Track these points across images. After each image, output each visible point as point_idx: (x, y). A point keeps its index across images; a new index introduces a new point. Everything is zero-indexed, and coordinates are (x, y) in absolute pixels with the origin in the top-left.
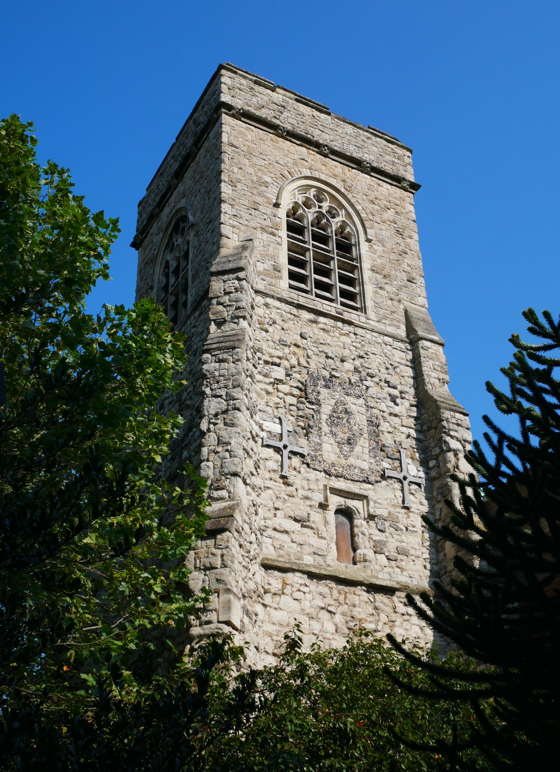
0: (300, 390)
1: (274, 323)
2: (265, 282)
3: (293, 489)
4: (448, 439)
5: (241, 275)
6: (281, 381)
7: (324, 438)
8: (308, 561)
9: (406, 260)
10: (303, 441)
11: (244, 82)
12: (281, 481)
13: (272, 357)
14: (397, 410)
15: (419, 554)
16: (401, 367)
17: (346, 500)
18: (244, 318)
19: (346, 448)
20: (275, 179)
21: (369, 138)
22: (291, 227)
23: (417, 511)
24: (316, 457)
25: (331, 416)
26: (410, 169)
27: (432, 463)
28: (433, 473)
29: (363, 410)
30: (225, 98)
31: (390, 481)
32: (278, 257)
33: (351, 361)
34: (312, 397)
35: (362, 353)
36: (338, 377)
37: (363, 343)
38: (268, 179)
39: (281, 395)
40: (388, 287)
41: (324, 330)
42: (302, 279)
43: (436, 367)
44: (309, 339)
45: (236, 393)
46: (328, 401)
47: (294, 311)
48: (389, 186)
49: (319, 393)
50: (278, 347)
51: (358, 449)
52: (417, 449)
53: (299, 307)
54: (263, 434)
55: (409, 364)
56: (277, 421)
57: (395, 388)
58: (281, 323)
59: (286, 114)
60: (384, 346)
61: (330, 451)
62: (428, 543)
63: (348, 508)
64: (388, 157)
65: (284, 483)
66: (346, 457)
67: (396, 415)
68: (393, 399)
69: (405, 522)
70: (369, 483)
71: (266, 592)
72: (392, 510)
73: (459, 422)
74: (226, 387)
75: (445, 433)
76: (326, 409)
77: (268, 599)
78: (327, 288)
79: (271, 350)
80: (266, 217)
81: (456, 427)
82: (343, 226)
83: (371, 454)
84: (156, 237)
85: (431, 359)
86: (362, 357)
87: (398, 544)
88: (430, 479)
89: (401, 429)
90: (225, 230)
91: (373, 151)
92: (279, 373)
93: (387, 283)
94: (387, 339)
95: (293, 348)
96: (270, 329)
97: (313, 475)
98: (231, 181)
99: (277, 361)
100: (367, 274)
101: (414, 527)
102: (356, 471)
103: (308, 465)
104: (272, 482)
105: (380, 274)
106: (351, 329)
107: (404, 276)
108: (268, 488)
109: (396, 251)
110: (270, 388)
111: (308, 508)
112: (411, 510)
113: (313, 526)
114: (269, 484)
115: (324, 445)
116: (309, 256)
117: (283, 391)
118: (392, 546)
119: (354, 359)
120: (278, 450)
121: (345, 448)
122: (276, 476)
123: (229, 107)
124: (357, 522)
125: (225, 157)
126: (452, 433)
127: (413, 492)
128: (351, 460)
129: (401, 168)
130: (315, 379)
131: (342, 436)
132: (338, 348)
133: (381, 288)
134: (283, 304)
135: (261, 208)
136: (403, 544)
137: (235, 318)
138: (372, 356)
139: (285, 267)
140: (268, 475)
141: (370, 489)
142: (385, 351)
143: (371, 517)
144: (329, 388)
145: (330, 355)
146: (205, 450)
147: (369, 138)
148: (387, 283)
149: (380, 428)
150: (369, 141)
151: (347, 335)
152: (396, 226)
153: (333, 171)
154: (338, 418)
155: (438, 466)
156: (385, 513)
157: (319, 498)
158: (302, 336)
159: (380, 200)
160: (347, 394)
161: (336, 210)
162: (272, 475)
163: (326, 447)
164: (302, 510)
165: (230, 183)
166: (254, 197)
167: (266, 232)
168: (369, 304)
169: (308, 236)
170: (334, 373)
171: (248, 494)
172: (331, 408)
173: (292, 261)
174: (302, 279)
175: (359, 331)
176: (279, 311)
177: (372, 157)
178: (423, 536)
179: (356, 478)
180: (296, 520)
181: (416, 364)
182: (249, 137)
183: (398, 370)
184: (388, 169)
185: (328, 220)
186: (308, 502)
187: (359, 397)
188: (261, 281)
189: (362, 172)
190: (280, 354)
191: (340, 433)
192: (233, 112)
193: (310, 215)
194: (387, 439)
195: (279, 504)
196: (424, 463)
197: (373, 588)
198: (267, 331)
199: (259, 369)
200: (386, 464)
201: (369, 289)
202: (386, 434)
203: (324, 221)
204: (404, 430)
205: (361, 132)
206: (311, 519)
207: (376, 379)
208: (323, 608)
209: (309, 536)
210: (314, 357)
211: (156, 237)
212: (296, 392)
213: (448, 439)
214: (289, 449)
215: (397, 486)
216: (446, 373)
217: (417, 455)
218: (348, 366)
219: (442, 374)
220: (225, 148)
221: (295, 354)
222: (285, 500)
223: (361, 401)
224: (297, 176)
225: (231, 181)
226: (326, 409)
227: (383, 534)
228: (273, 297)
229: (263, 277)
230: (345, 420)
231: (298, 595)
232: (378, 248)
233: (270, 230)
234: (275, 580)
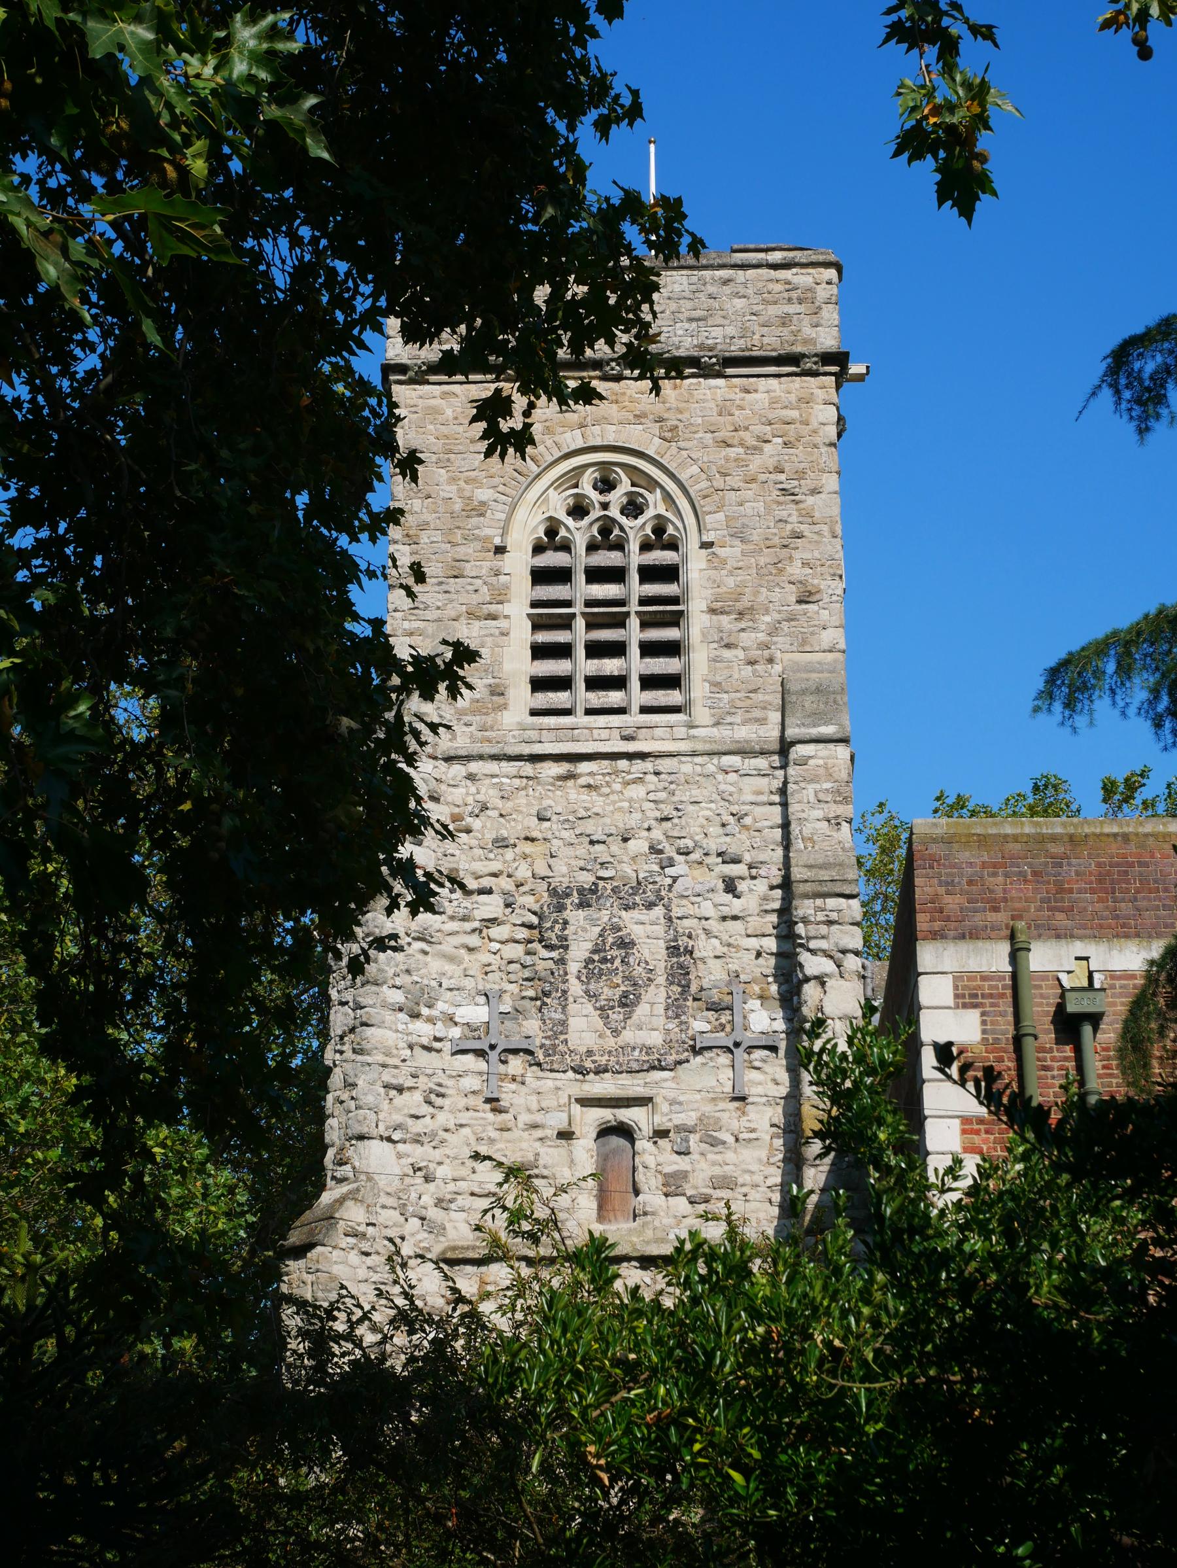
0: (530, 927)
1: (484, 808)
2: (472, 729)
3: (509, 1116)
6: (493, 921)
7: (572, 1008)
9: (797, 555)
12: (488, 1106)
15: (758, 1178)
16: (759, 811)
17: (616, 1111)
19: (616, 1016)
20: (501, 488)
21: (726, 282)
22: (540, 576)
23: (764, 1099)
24: (555, 1046)
25: (589, 961)
29: (659, 930)
31: (708, 1054)
32: (501, 663)
33: (645, 834)
35: (668, 810)
36: (611, 878)
37: (673, 786)
38: (484, 494)
39: (496, 946)
40: (747, 639)
41: (589, 786)
43: (822, 796)
44: (554, 818)
46: (583, 931)
47: (528, 769)
48: (773, 382)
49: (566, 923)
50: (491, 856)
51: (642, 1010)
52: (775, 976)
54: (456, 1032)
55: (777, 798)
56: (482, 999)
58: (499, 803)
60: (720, 777)
61: (584, 1028)
62: (781, 1156)
63: (622, 1123)
64: (773, 310)
65: (493, 1110)
66: (616, 1032)
68: (730, 886)
69: (735, 1125)
70: (663, 1069)
72: (708, 1108)
73: (834, 916)
75: (802, 945)
76: (579, 951)
80: (479, 582)
81: (824, 929)
83: (670, 1013)
85: (812, 781)
87: (717, 1171)
92: (491, 906)
93: (743, 630)
94: (727, 760)
96: (476, 824)
97: (549, 1082)
98: (407, 535)
99: (486, 882)
101: (753, 1131)
102: (636, 1053)
103: (539, 1065)
104: (471, 1113)
105: (727, 613)
106: (648, 765)
107: (791, 594)
108: (461, 1126)
109: (776, 541)
110: (474, 940)
111: (538, 1144)
112: (750, 1100)
113: (545, 1172)
114: (464, 1117)
115: (572, 1022)
117: (498, 938)
119: (649, 829)
120: (480, 1053)
121: (615, 1016)
122: (478, 1101)
124: (639, 1145)
126: (813, 945)
127: (757, 1064)
128: (628, 1036)
129: (806, 320)
130: (559, 897)
132: (617, 816)
133: (728, 646)
134: (504, 764)
135: (469, 569)
136: (726, 1168)
138: (691, 808)
140: (462, 1102)
141: (666, 1080)
142: (722, 787)
144: (589, 906)
147: (726, 282)
148: (743, 630)
149: (697, 954)
150: (727, 290)
151: (639, 780)
152: (782, 477)
154: (604, 960)
157: (558, 1121)
159: (747, 429)
160: (627, 908)
161: (642, 495)
162: (473, 1101)
163: (576, 1024)
165: (406, 540)
166: (458, 549)
167: (478, 618)
170: (602, 873)
171: (400, 1156)
172: (589, 946)
175: (665, 765)
176: (495, 780)
177: (731, 331)
178: (771, 1145)
179: (635, 1066)
182: (449, 413)
183: (748, 821)
184: (771, 341)
185: (622, 529)
186: (539, 1133)
187: (650, 906)
188: (465, 729)
189: (706, 376)
190: (495, 866)
191: (606, 989)
192: (411, 374)
199: (450, 912)
202: (712, 963)
203: (616, 532)
204: (754, 943)
205: (707, 274)
206: (541, 1162)
212: (523, 934)
214: (499, 1049)
215: (724, 1059)
217: (774, 988)
218: (638, 845)
219: (834, 807)
221: (525, 856)
222: (492, 1141)
223: (659, 911)
224: (550, 459)
225: (407, 535)
226: (579, 951)
227: (686, 1158)
228: (481, 757)
229: (467, 718)
230: (617, 962)
232: (730, 552)
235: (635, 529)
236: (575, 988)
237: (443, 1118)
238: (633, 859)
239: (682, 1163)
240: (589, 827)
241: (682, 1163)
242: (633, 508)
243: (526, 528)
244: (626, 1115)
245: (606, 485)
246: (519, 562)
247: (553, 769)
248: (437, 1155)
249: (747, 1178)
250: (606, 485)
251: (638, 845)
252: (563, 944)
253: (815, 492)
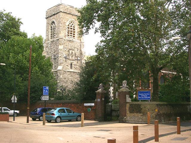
14: (78, 51)
46: (71, 51)
61: (70, 57)
76: (70, 53)
92: (66, 49)
116: (70, 32)
139: (67, 34)
174: (69, 35)
218: (73, 47)
226: (70, 53)
235: (73, 26)
238: (73, 48)
242: (73, 24)
244: (72, 63)
245: (71, 22)
250: (71, 22)
251: (73, 47)
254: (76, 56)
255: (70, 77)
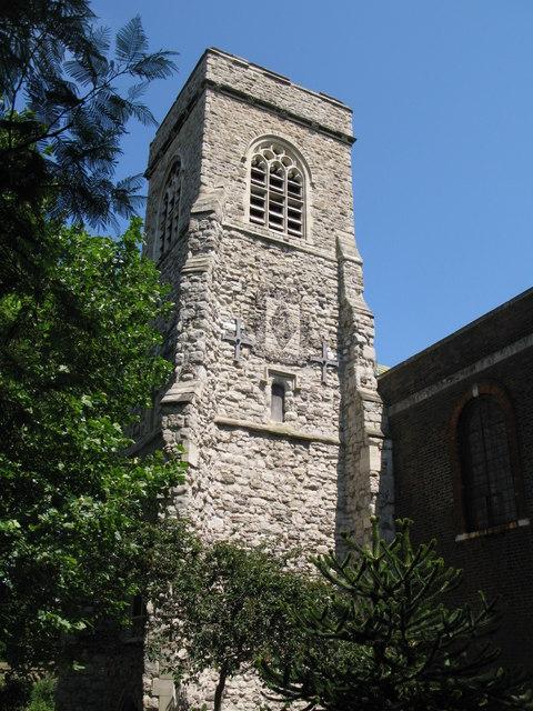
4: (356, 334)
5: (212, 216)
6: (238, 293)
8: (250, 422)
10: (252, 336)
11: (224, 62)
13: (232, 274)
14: (323, 312)
18: (212, 248)
19: (283, 340)
22: (254, 175)
26: (350, 125)
27: (345, 351)
28: (345, 358)
29: (298, 313)
30: (210, 76)
34: (261, 304)
35: (300, 271)
42: (260, 214)
45: (201, 304)
46: (272, 305)
53: (256, 237)
54: (223, 332)
57: (323, 296)
59: (256, 86)
61: (271, 343)
67: (322, 316)
71: (219, 441)
74: (196, 300)
76: (270, 313)
77: (219, 446)
78: (279, 221)
79: (232, 270)
82: (294, 172)
84: (160, 175)
86: (300, 274)
88: (343, 364)
89: (326, 330)
90: (204, 179)
91: (320, 113)
95: (249, 268)
96: (233, 254)
97: (257, 360)
100: (309, 209)
110: (230, 298)
114: (225, 367)
116: (267, 198)
118: (311, 408)
120: (232, 343)
123: (212, 84)
125: (207, 123)
128: (286, 349)
131: (280, 331)
137: (206, 250)
139: (247, 205)
143: (297, 392)
145: (276, 272)
146: (179, 345)
153: (288, 131)
155: (349, 354)
156: (308, 387)
158: (257, 259)
164: (247, 385)
168: (309, 232)
169: (266, 182)
171: (208, 375)
173: (253, 201)
174: (260, 214)
180: (243, 393)
181: (340, 277)
184: (332, 126)
187: (295, 303)
190: (239, 272)
193: (270, 164)
194: (315, 335)
195: (231, 381)
196: (339, 351)
197: (294, 440)
198: (230, 256)
200: (311, 351)
201: (310, 222)
207: (310, 290)
208: (257, 452)
209: (254, 405)
210: (264, 274)
211: (160, 175)
212: (249, 301)
213: (356, 334)
216: (362, 285)
218: (289, 279)
220: (208, 115)
222: (236, 379)
223: (297, 306)
226: (270, 313)
231: (240, 443)
233: (238, 178)
234: (225, 435)
236: (269, 327)
237: (218, 365)
239: (304, 404)
240: (273, 268)
241: (304, 404)
243: (250, 156)
246: (248, 165)
247: (259, 243)
248: (217, 379)
249: (325, 413)
252: (264, 308)
253: (346, 180)
254: (315, 335)
255: (268, 475)
